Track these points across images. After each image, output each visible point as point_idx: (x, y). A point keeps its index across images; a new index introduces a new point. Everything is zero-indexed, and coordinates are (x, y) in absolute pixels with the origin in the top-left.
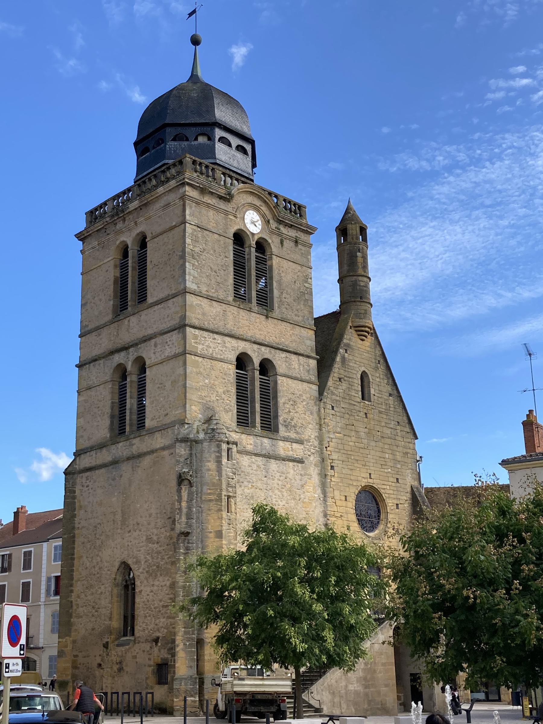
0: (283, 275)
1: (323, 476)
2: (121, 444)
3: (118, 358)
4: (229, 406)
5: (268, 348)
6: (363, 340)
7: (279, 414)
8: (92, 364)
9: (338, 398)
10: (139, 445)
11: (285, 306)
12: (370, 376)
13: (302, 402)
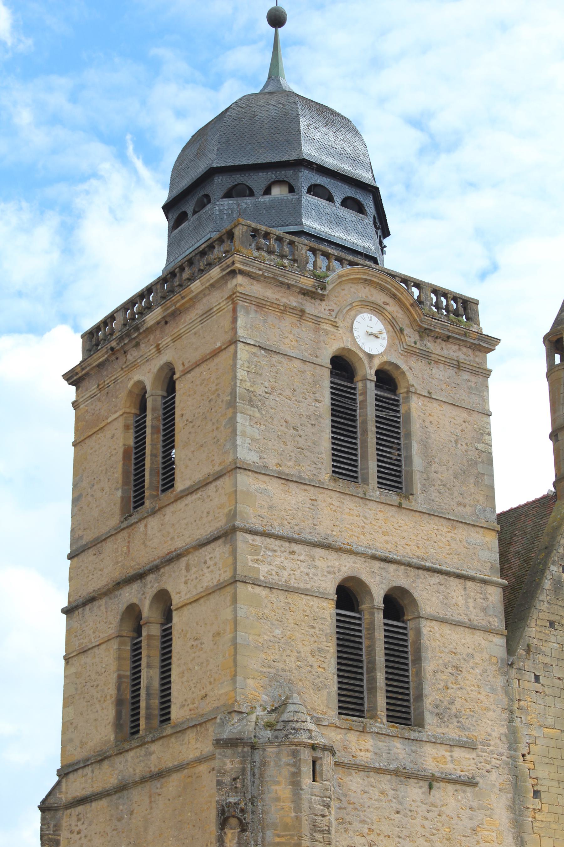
0: (431, 429)
1: (517, 810)
2: (131, 754)
3: (129, 595)
4: (321, 679)
5: (402, 567)
7: (425, 692)
8: (87, 607)
9: (548, 660)
10: (161, 754)
11: (437, 487)
13: (472, 668)
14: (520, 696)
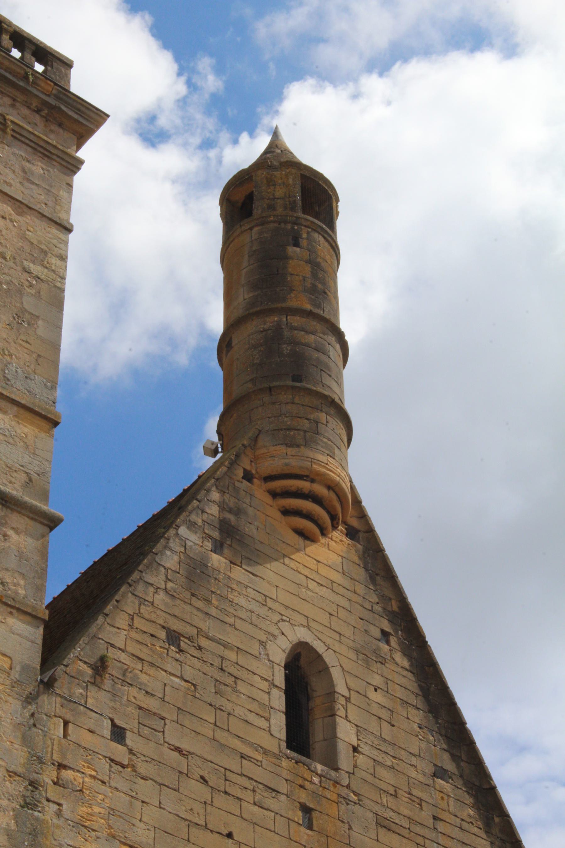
6: (301, 533)
9: (152, 704)
12: (336, 673)
14: (63, 753)
